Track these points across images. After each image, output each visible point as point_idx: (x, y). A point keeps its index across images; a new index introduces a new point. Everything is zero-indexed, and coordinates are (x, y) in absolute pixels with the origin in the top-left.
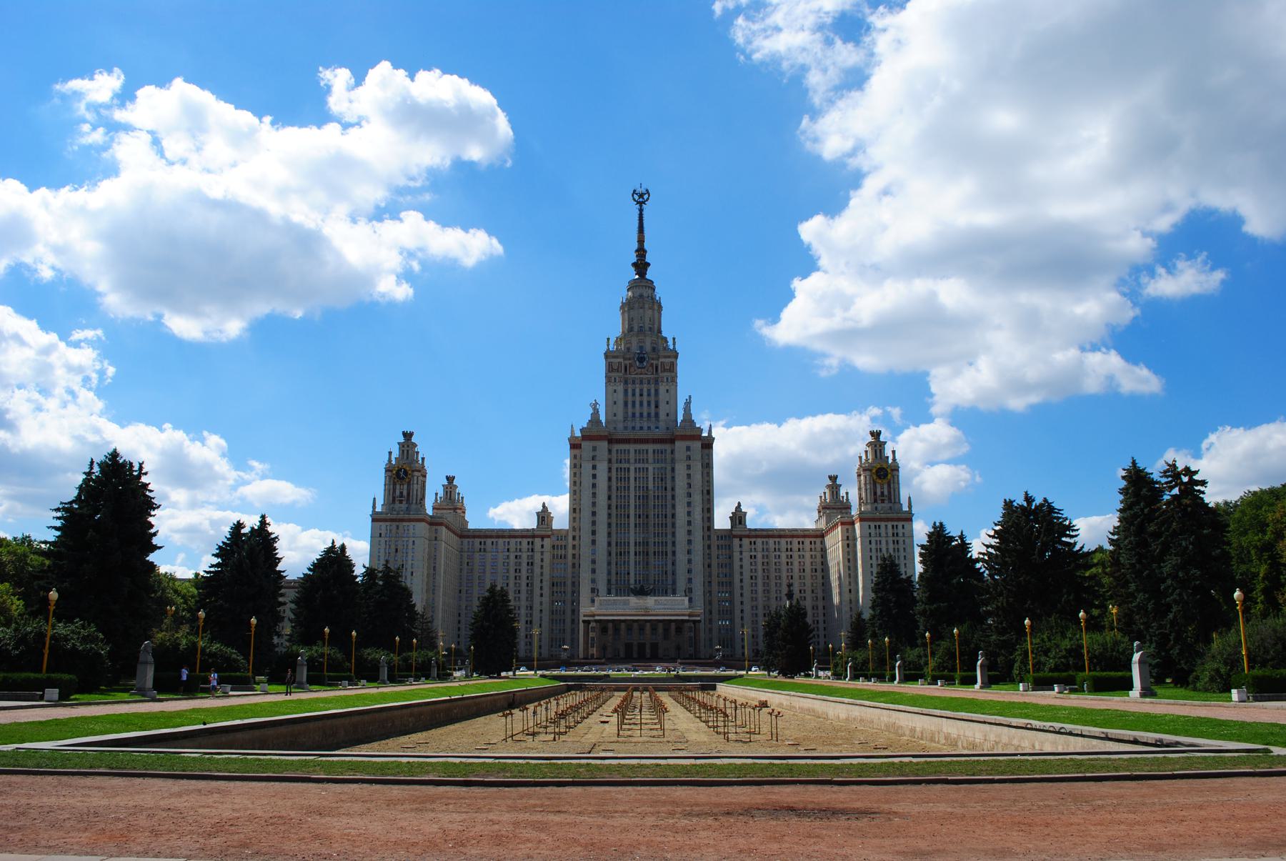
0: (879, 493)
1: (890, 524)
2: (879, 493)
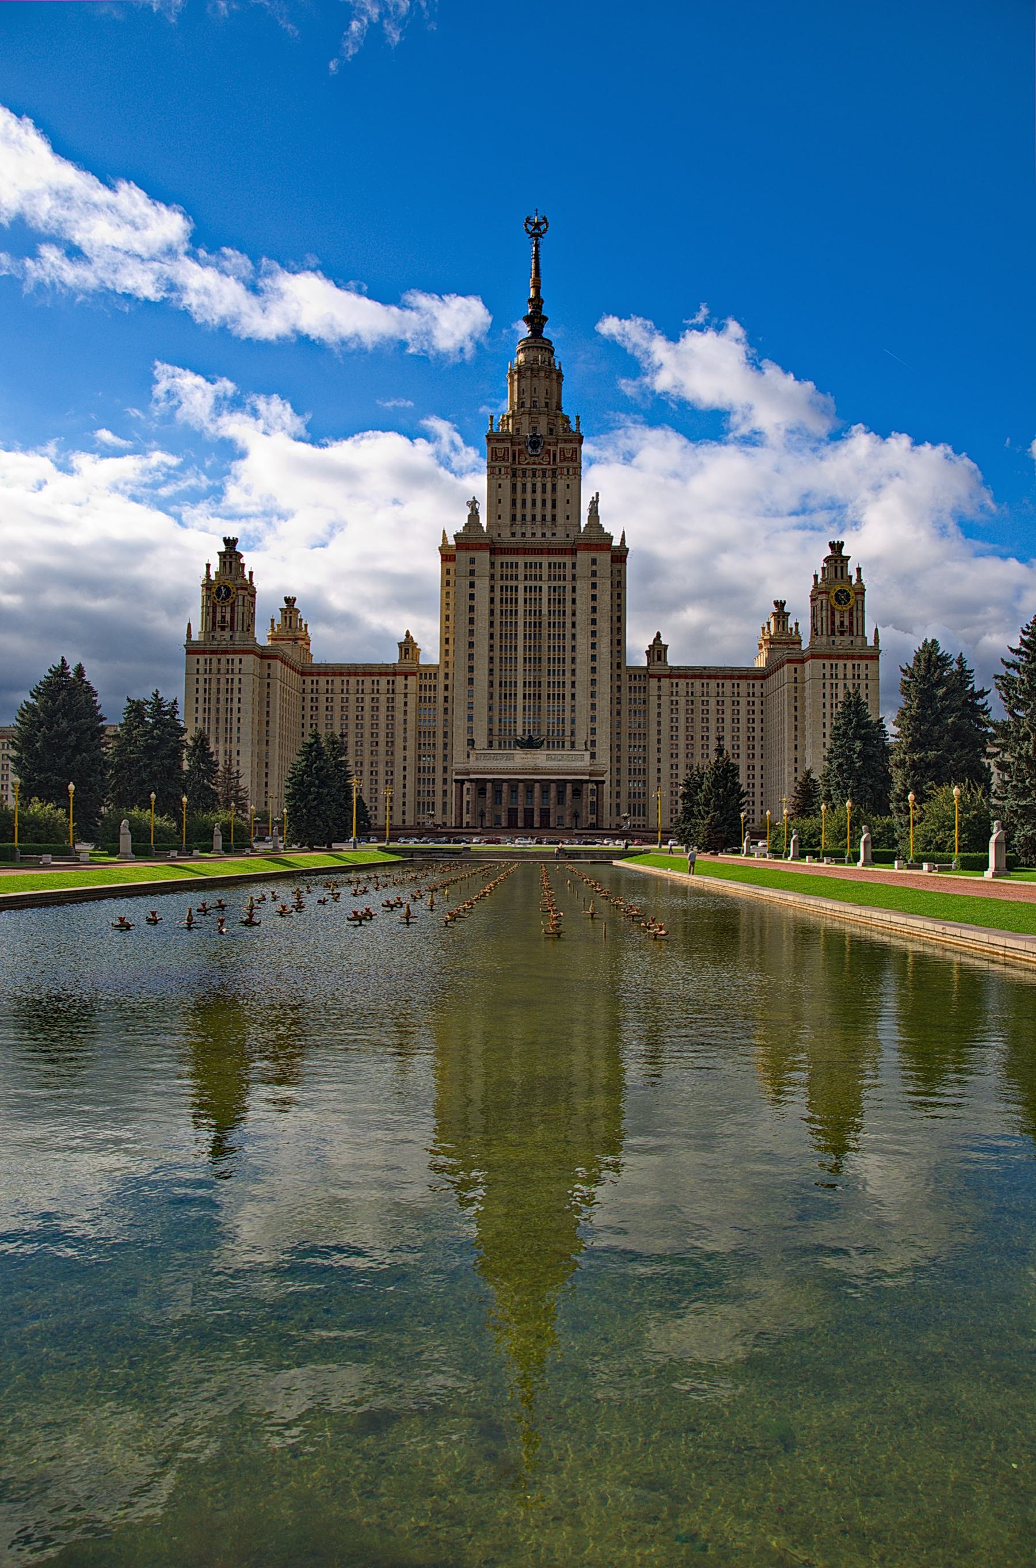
0: (837, 623)
1: (849, 663)
2: (837, 623)
